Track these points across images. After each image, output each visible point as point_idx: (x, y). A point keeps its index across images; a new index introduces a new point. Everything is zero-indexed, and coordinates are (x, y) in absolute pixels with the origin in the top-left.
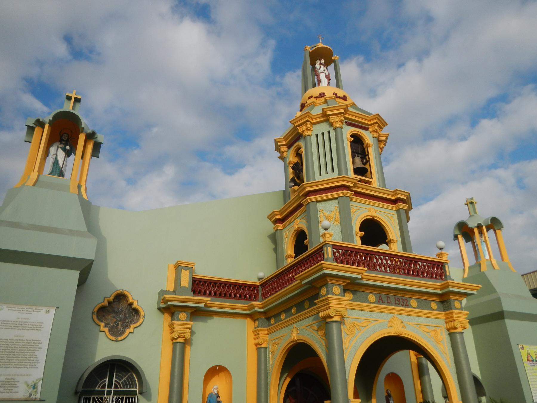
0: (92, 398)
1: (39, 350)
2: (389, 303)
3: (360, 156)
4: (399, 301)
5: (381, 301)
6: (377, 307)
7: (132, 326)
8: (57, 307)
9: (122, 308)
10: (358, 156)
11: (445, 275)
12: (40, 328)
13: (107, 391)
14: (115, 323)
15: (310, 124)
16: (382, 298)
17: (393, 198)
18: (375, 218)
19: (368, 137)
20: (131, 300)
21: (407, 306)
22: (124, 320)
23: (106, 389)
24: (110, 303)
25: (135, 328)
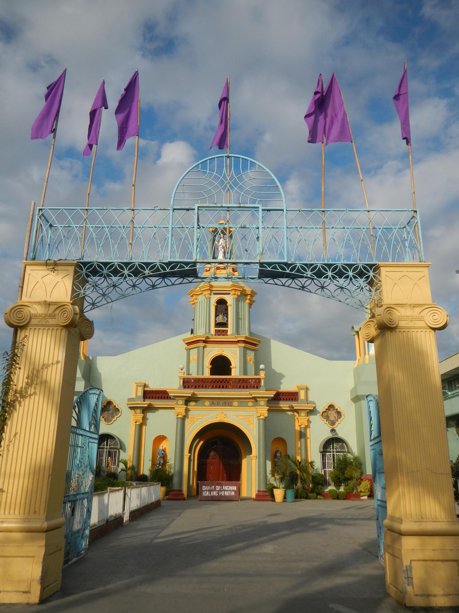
4: (226, 404)
5: (213, 405)
6: (210, 408)
7: (116, 417)
11: (260, 386)
13: (106, 448)
14: (108, 415)
15: (195, 296)
17: (236, 340)
18: (223, 355)
19: (230, 300)
20: (114, 404)
21: (231, 406)
22: (113, 413)
23: (105, 447)
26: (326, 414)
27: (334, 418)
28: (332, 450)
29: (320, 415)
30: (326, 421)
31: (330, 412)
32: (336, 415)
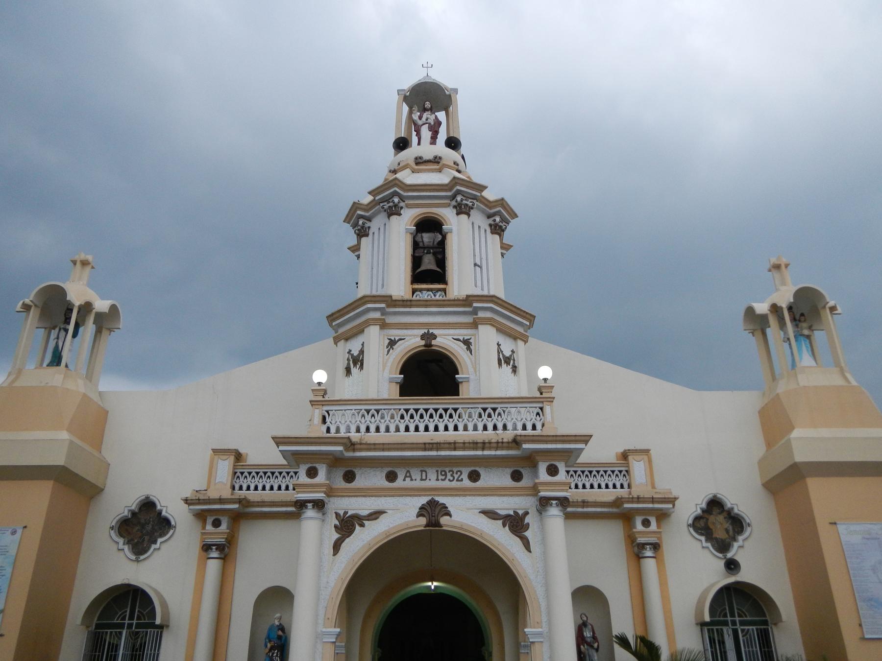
0: (109, 632)
1: (4, 577)
2: (425, 480)
3: (432, 251)
4: (446, 475)
7: (160, 540)
8: (24, 525)
9: (150, 518)
10: (427, 253)
12: (5, 552)
13: (128, 624)
14: (140, 537)
16: (411, 472)
23: (127, 622)
24: (134, 514)
25: (161, 543)
26: (702, 523)
27: (725, 533)
28: (729, 619)
29: (688, 525)
30: (706, 541)
31: (712, 518)
32: (728, 525)
